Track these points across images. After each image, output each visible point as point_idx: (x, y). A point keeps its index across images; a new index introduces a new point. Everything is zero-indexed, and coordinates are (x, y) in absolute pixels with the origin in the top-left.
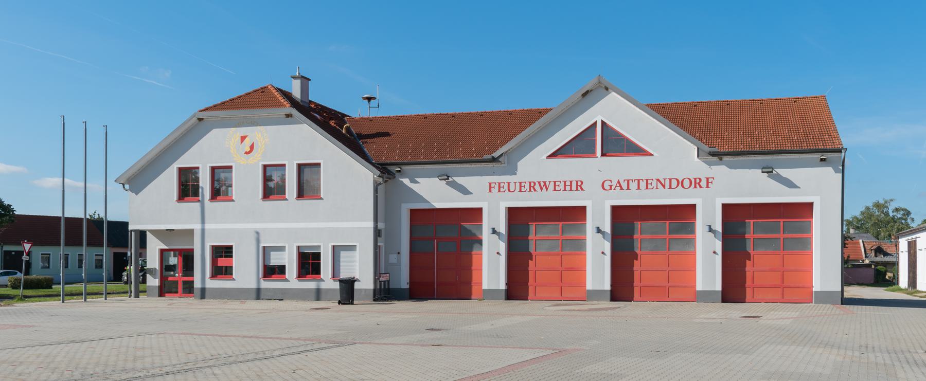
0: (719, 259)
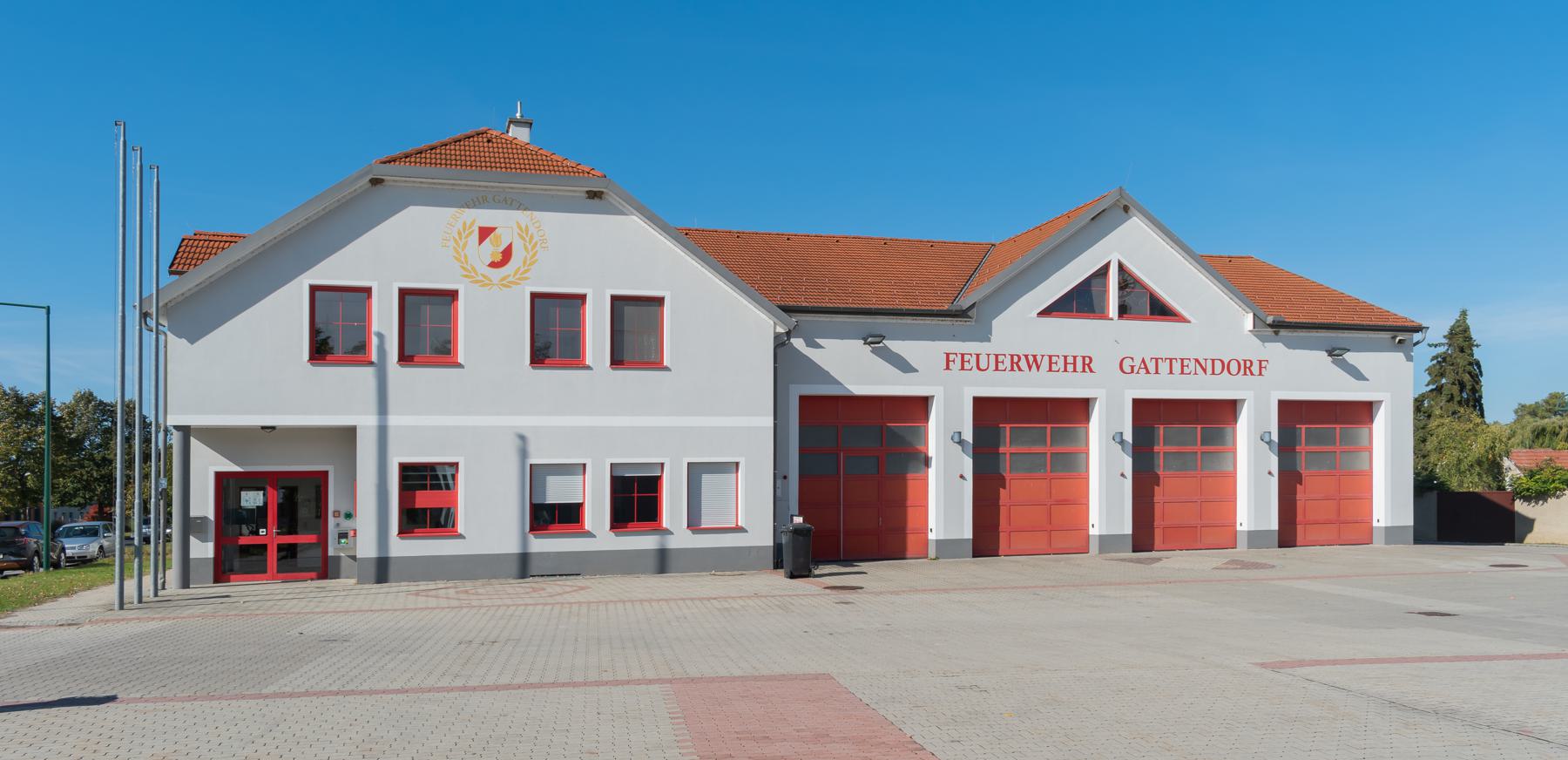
0: (1128, 484)
